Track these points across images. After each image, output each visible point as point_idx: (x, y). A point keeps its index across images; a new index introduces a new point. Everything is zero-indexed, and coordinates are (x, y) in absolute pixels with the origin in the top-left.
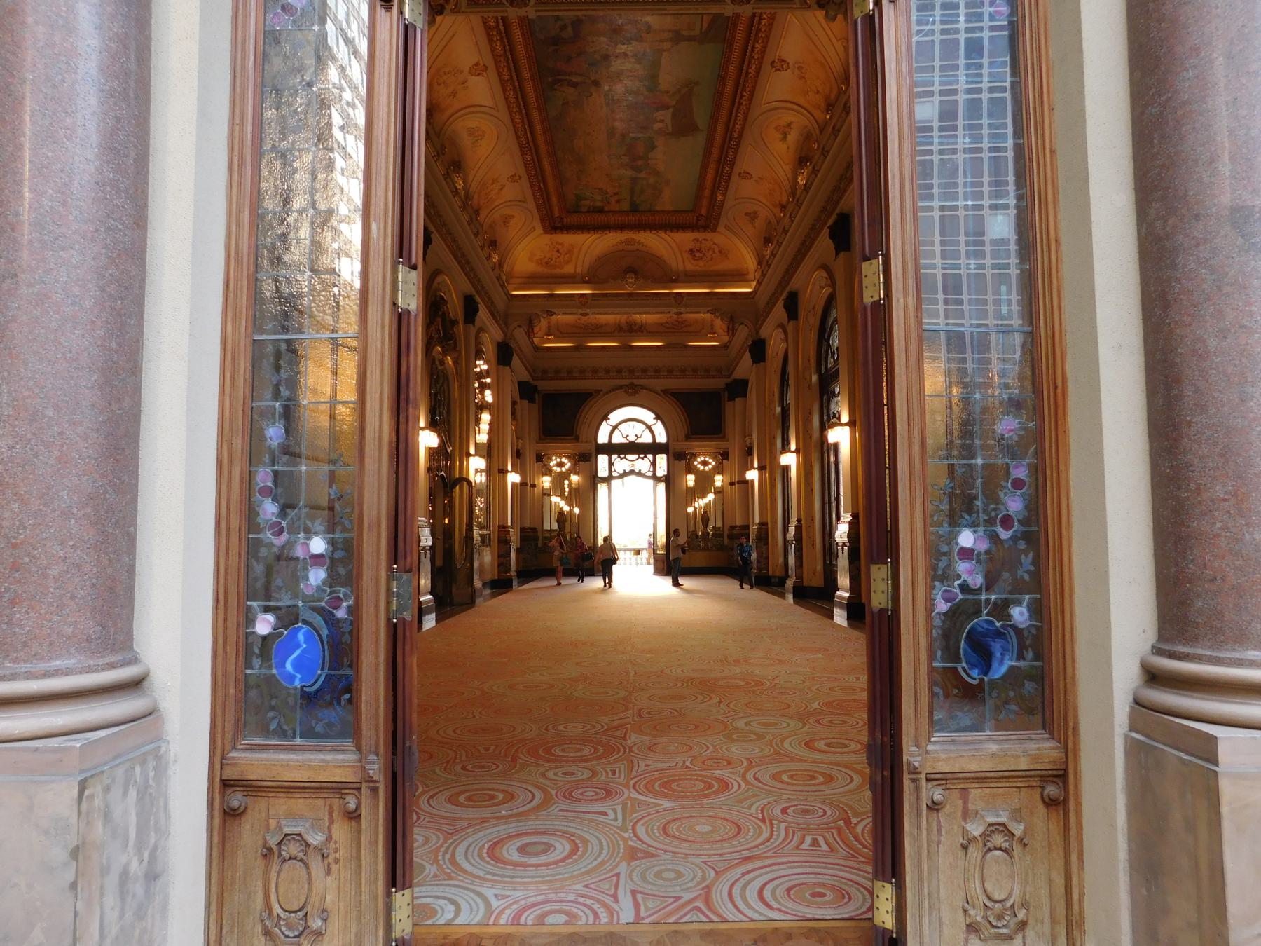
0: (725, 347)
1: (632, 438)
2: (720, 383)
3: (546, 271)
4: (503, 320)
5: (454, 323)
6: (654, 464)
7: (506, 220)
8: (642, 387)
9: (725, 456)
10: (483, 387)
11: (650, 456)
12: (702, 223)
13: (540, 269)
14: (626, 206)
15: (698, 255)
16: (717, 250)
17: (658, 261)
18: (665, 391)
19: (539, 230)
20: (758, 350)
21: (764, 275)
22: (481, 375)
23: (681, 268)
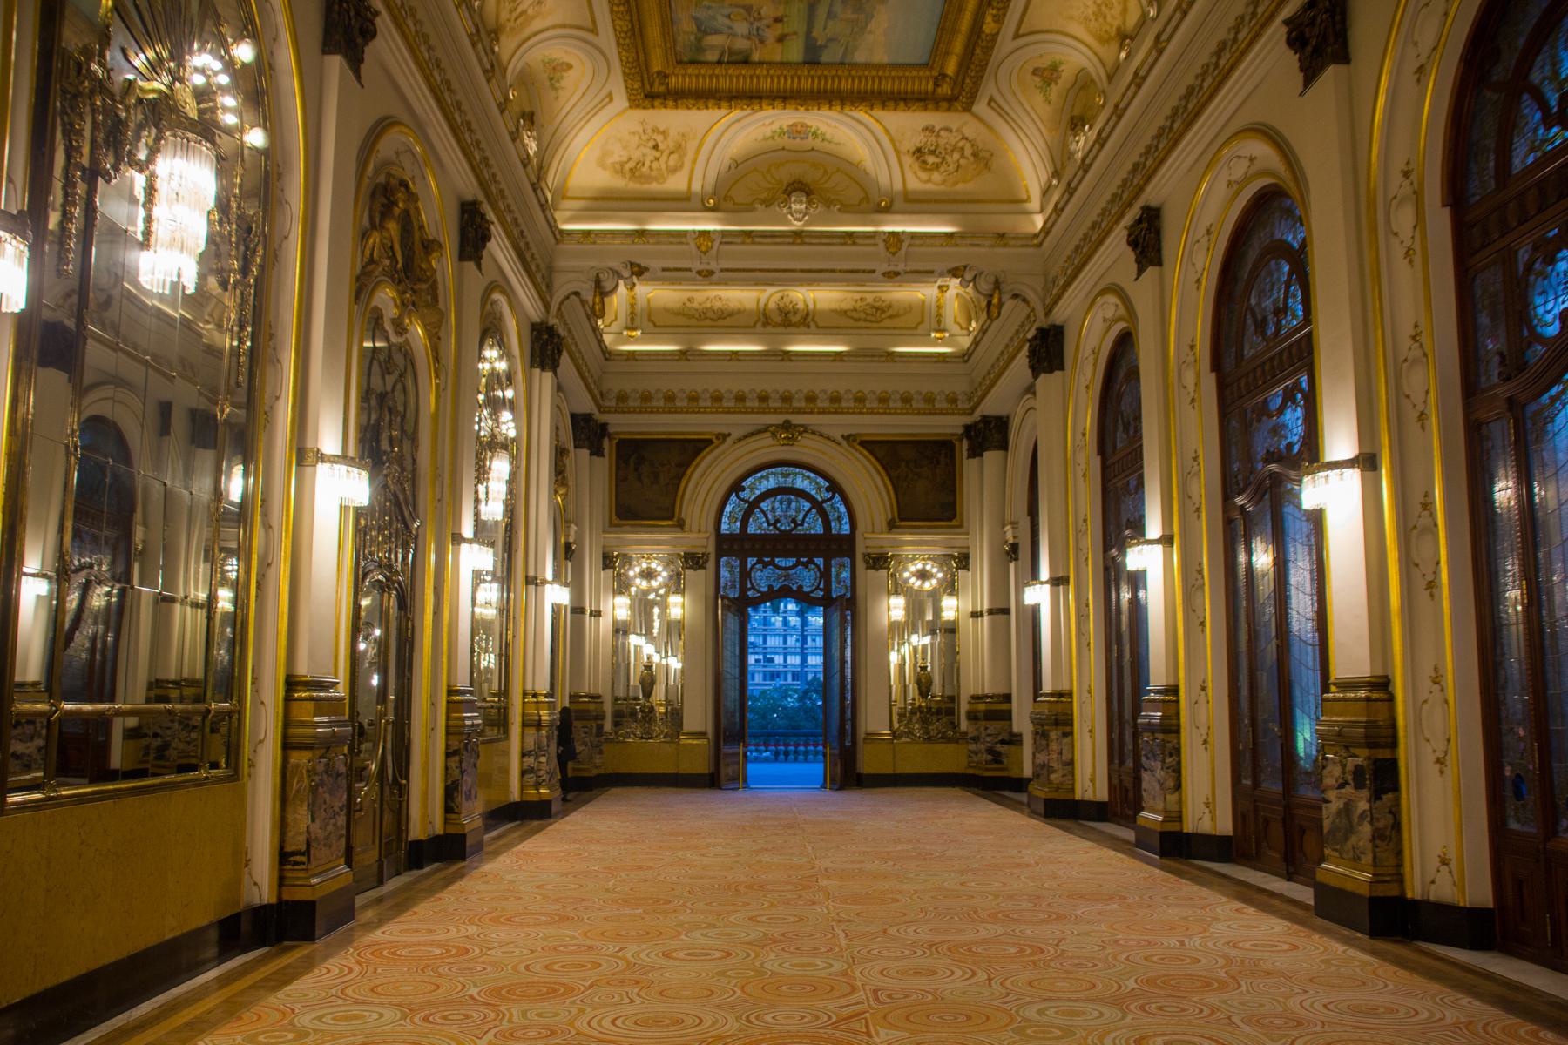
0: (965, 356)
1: (785, 527)
2: (949, 425)
3: (633, 186)
4: (540, 273)
5: (430, 246)
6: (825, 575)
7: (557, 70)
8: (805, 429)
9: (963, 561)
10: (496, 405)
11: (820, 561)
12: (945, 89)
13: (620, 183)
14: (795, 52)
15: (931, 159)
16: (968, 152)
17: (850, 170)
18: (847, 438)
19: (621, 101)
20: (1048, 350)
21: (1070, 191)
22: (495, 379)
23: (898, 186)
